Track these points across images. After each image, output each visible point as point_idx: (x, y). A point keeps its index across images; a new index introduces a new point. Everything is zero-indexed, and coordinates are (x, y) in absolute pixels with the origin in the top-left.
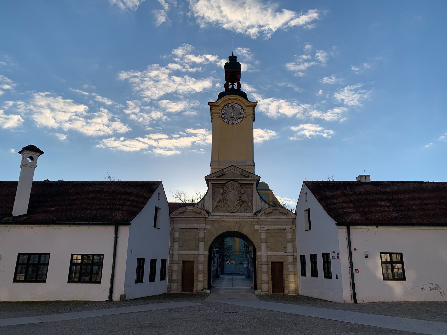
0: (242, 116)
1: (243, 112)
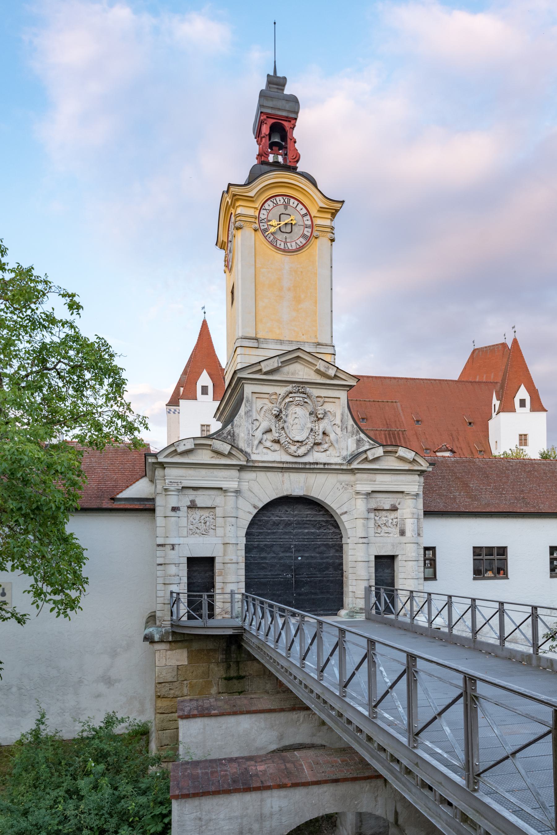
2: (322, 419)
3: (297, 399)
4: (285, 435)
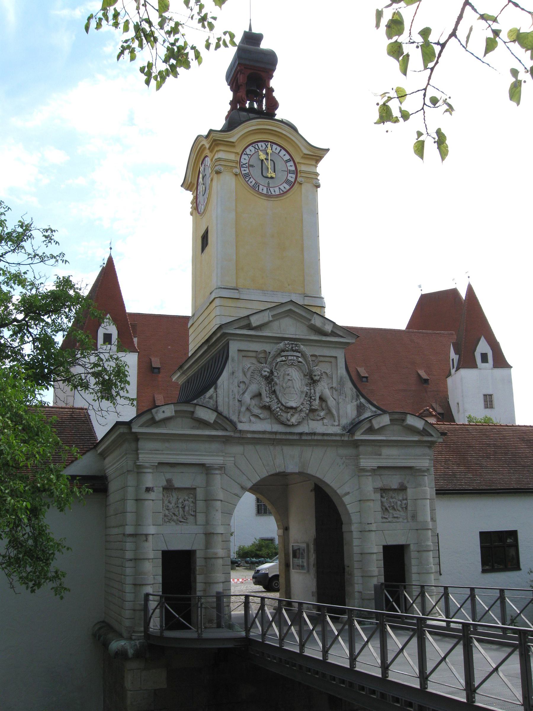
0: (291, 177)
1: (293, 168)
2: (318, 381)
3: (290, 358)
4: (276, 401)
